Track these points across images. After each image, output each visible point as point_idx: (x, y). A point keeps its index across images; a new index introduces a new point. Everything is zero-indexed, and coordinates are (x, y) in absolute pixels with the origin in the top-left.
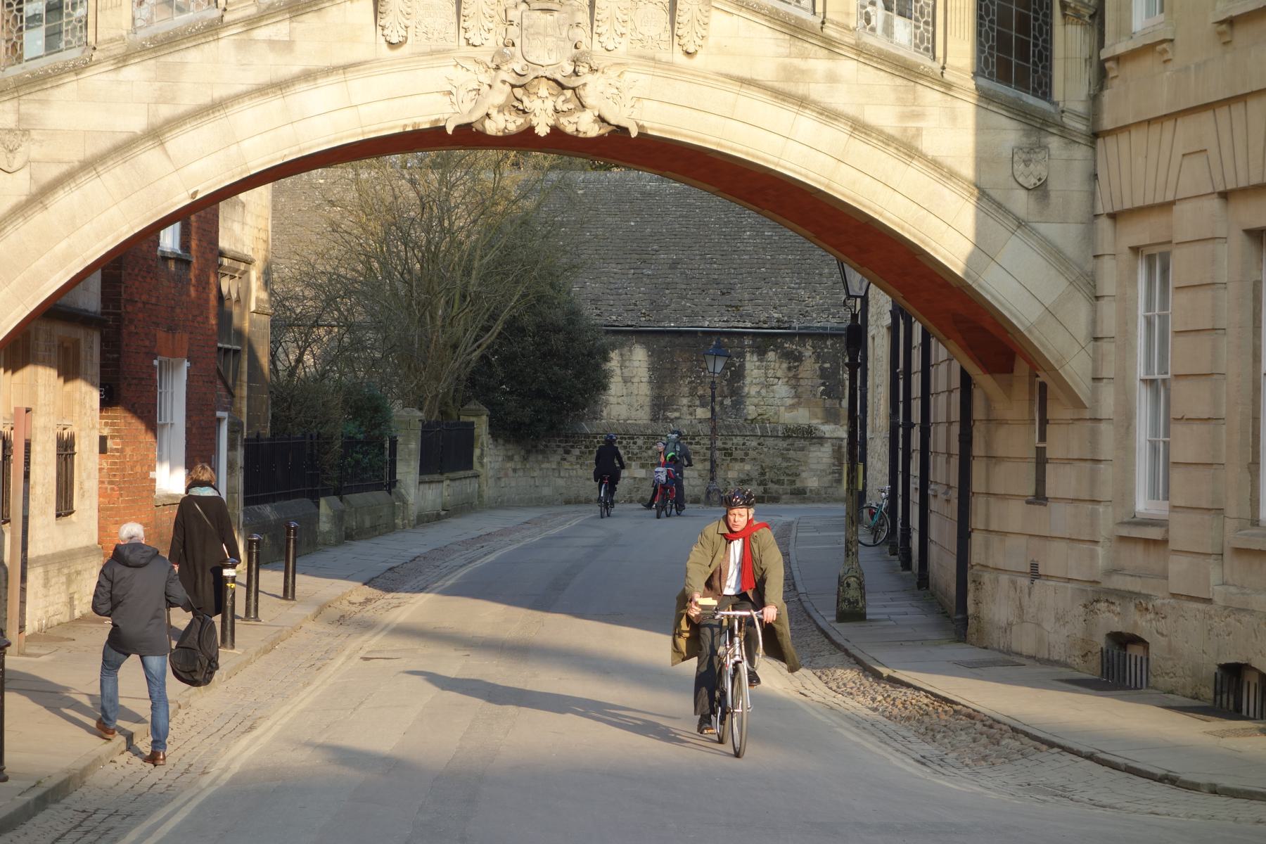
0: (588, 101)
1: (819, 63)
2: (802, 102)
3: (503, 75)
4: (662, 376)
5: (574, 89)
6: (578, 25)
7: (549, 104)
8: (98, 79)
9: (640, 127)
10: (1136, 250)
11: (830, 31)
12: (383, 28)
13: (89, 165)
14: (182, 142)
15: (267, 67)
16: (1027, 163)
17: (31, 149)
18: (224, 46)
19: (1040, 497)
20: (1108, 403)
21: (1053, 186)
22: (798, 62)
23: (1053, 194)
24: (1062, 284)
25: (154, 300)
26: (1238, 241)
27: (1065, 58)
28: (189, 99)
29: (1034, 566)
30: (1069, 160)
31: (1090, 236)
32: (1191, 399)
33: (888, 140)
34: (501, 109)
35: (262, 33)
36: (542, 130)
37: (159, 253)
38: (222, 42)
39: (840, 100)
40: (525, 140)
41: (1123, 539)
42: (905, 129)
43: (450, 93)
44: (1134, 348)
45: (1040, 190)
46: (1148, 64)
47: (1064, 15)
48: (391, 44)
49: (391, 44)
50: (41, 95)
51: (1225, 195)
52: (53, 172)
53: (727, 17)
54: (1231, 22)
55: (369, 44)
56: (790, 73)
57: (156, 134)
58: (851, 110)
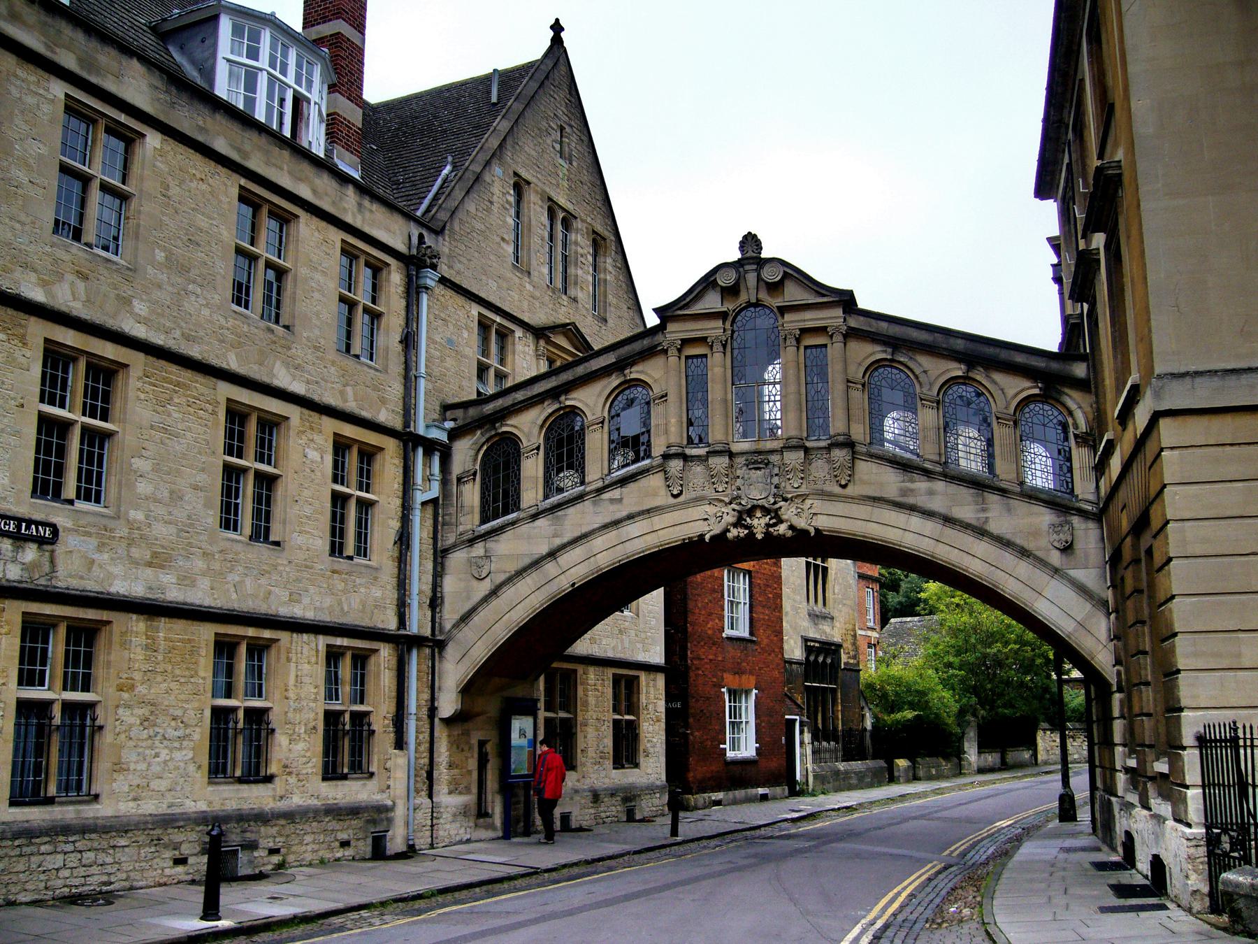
0: (784, 517)
1: (922, 485)
2: (912, 508)
3: (733, 506)
5: (776, 511)
6: (776, 475)
8: (524, 529)
9: (817, 530)
11: (928, 465)
12: (669, 486)
13: (520, 573)
14: (566, 559)
15: (607, 512)
16: (1058, 533)
18: (587, 505)
21: (1078, 546)
23: (1077, 552)
25: (720, 659)
30: (1087, 529)
34: (735, 525)
35: (606, 496)
36: (759, 536)
37: (724, 635)
39: (936, 505)
42: (978, 519)
43: (706, 519)
45: (1067, 549)
47: (1077, 442)
50: (496, 538)
52: (501, 578)
53: (862, 463)
55: (663, 499)
57: (552, 554)
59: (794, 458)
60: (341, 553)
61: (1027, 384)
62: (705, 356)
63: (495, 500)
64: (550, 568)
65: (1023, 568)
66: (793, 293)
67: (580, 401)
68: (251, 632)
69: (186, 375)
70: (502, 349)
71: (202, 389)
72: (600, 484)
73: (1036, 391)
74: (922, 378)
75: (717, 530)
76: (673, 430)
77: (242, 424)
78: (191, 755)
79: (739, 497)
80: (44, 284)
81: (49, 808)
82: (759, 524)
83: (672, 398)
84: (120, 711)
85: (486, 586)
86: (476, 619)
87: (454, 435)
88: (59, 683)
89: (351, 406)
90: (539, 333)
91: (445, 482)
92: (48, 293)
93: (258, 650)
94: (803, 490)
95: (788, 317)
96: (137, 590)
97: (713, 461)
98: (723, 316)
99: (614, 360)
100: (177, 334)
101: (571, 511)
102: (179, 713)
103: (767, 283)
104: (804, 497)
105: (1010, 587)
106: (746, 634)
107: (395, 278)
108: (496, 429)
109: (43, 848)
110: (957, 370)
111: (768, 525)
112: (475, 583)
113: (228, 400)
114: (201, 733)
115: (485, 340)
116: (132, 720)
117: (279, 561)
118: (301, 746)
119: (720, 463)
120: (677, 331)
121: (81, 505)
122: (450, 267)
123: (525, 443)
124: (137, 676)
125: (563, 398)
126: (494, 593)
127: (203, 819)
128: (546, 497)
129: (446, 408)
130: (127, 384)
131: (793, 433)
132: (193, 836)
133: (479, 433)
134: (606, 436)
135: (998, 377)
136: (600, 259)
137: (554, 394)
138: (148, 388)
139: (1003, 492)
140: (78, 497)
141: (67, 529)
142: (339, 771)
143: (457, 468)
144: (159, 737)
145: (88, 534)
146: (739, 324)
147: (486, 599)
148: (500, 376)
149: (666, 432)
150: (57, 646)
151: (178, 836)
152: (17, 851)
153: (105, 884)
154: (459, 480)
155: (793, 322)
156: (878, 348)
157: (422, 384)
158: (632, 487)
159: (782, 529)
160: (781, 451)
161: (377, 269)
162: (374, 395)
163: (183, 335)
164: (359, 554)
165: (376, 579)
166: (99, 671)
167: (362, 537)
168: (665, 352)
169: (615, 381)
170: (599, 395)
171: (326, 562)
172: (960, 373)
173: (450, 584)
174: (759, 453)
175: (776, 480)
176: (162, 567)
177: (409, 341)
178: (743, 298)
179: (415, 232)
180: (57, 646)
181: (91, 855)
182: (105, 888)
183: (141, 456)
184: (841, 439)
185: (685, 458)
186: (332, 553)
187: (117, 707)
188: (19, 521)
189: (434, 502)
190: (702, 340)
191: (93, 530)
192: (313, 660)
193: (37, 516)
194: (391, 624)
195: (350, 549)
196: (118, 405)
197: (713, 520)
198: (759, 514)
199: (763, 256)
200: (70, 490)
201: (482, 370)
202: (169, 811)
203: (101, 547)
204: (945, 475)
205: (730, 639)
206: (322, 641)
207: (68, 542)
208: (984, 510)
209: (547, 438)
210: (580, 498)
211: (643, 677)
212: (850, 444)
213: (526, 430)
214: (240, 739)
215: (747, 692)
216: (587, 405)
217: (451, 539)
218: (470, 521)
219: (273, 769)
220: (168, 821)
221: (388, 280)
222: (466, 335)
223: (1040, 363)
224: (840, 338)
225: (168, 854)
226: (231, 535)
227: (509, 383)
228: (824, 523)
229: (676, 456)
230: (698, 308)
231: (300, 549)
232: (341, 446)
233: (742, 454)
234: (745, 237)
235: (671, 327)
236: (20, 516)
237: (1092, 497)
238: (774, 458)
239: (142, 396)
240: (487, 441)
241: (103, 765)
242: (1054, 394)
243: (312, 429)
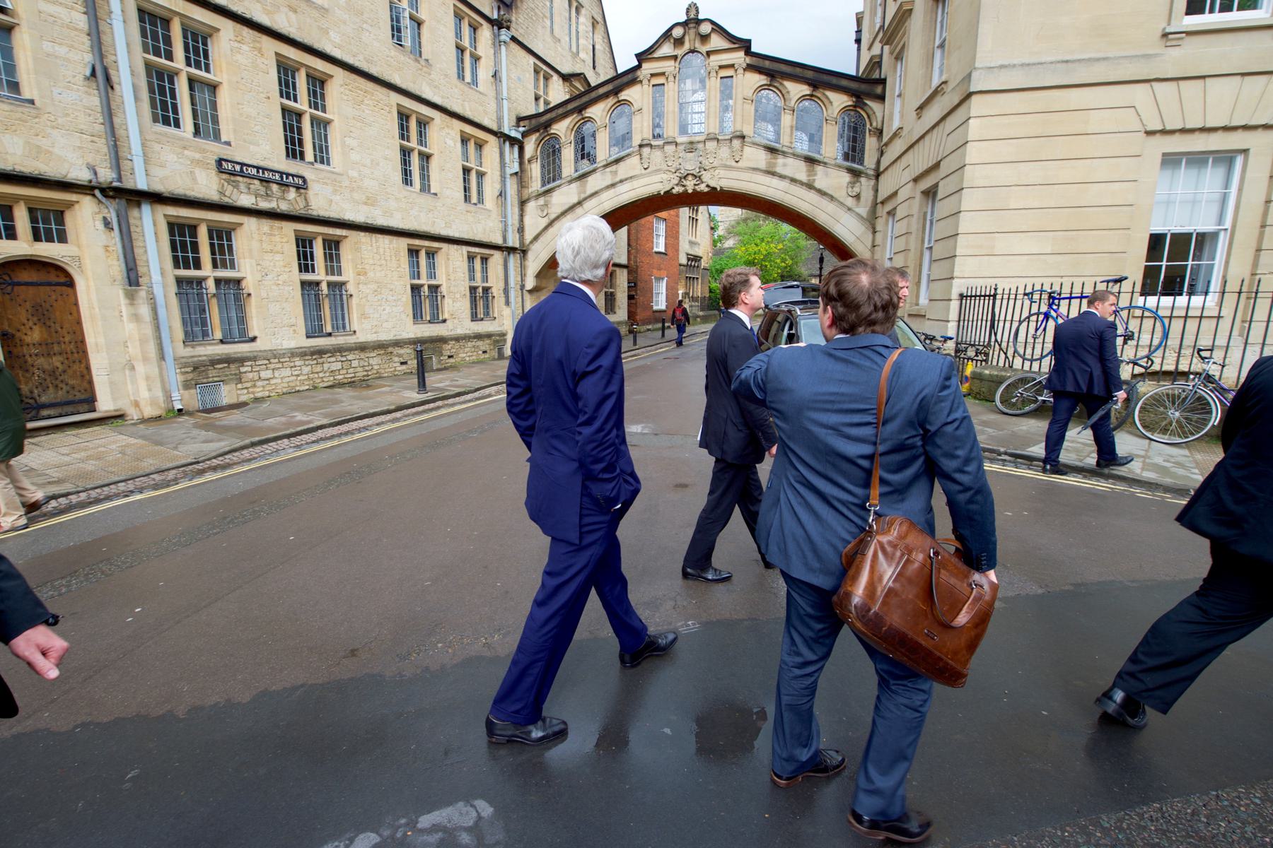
0: (704, 180)
2: (773, 174)
3: (677, 174)
8: (564, 189)
22: (773, 161)
28: (588, 193)
33: (802, 183)
34: (677, 185)
35: (608, 170)
36: (690, 191)
38: (598, 174)
48: (645, 169)
49: (645, 169)
55: (638, 170)
56: (769, 164)
57: (580, 203)
58: (790, 175)
59: (711, 145)
60: (470, 201)
63: (549, 173)
65: (830, 207)
68: (427, 243)
69: (370, 86)
70: (546, 86)
71: (381, 96)
72: (605, 163)
76: (645, 130)
77: (407, 122)
78: (402, 309)
79: (680, 169)
81: (329, 338)
82: (690, 185)
83: (645, 110)
84: (361, 286)
86: (542, 239)
87: (524, 135)
88: (323, 271)
89: (468, 114)
90: (566, 78)
91: (521, 163)
93: (431, 254)
94: (713, 165)
96: (359, 218)
97: (667, 148)
98: (675, 58)
100: (361, 58)
102: (392, 287)
109: (329, 360)
111: (695, 185)
113: (398, 104)
115: (537, 80)
116: (368, 291)
117: (437, 204)
118: (458, 305)
119: (670, 149)
120: (648, 68)
121: (318, 166)
122: (516, 30)
123: (563, 139)
124: (367, 267)
127: (414, 342)
128: (576, 171)
129: (520, 119)
131: (711, 130)
132: (408, 351)
133: (538, 134)
134: (607, 135)
136: (596, 36)
138: (347, 92)
140: (316, 161)
141: (313, 181)
142: (479, 316)
144: (384, 300)
145: (327, 184)
147: (546, 228)
148: (547, 103)
149: (642, 132)
150: (318, 250)
151: (402, 351)
152: (315, 362)
153: (364, 376)
158: (622, 164)
159: (703, 188)
161: (474, 28)
162: (481, 108)
164: (479, 202)
165: (489, 216)
166: (344, 264)
167: (480, 193)
168: (641, 82)
169: (611, 101)
170: (603, 111)
171: (462, 205)
173: (527, 220)
174: (691, 143)
176: (372, 205)
180: (318, 250)
181: (357, 362)
182: (366, 378)
183: (350, 137)
184: (738, 134)
185: (651, 146)
186: (466, 200)
187: (358, 284)
188: (281, 173)
189: (516, 173)
190: (663, 74)
191: (329, 182)
192: (461, 259)
195: (474, 199)
197: (665, 182)
198: (690, 178)
200: (309, 155)
201: (537, 99)
202: (395, 338)
203: (335, 191)
204: (794, 155)
206: (465, 249)
209: (575, 137)
212: (743, 137)
214: (427, 301)
216: (597, 116)
217: (525, 197)
218: (535, 185)
219: (446, 316)
220: (398, 344)
222: (527, 75)
223: (853, 85)
226: (409, 188)
227: (552, 105)
229: (647, 145)
230: (658, 54)
231: (448, 197)
232: (465, 140)
233: (682, 144)
235: (645, 65)
236: (281, 170)
238: (700, 146)
239: (345, 98)
243: (448, 126)
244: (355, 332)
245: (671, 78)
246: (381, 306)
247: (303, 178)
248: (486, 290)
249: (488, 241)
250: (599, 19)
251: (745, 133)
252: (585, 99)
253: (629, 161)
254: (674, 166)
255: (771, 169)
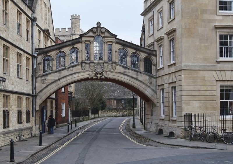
0: (104, 75)
1: (127, 71)
2: (126, 75)
4: (117, 103)
7: (99, 76)
8: (53, 74)
9: (109, 78)
10: (161, 89)
11: (129, 67)
14: (62, 80)
17: (46, 81)
18: (66, 71)
19: (152, 115)
20: (158, 105)
21: (152, 83)
22: (125, 71)
24: (153, 93)
26: (170, 88)
27: (153, 70)
28: (62, 76)
29: (152, 122)
31: (156, 88)
32: (166, 104)
34: (94, 76)
35: (70, 69)
36: (99, 78)
39: (130, 74)
40: (97, 79)
41: (160, 119)
44: (161, 99)
46: (161, 70)
51: (169, 83)
52: (48, 84)
54: (169, 66)
55: (81, 70)
56: (125, 72)
57: (59, 80)
58: (131, 75)
59: (106, 65)
61: (146, 54)
62: (89, 44)
64: (59, 82)
65: (143, 86)
66: (106, 34)
67: (64, 50)
68: (20, 96)
72: (69, 67)
73: (147, 56)
74: (128, 52)
75: (91, 77)
80: (3, 33)
82: (99, 76)
83: (83, 51)
85: (45, 85)
86: (43, 91)
87: (38, 55)
90: (44, 31)
92: (3, 36)
95: (105, 39)
98: (93, 37)
99: (71, 43)
101: (62, 71)
102: (15, 111)
103: (101, 31)
104: (107, 72)
105: (141, 89)
106: (63, 91)
107: (31, 24)
108: (47, 54)
109: (7, 136)
110: (134, 51)
111: (100, 76)
112: (43, 84)
114: (17, 115)
119: (92, 65)
120: (84, 39)
125: (61, 50)
126: (47, 86)
129: (36, 49)
130: (9, 51)
133: (43, 55)
135: (141, 53)
137: (59, 49)
139: (141, 73)
143: (38, 62)
146: (95, 39)
147: (45, 88)
149: (82, 58)
154: (39, 64)
155: (106, 39)
156: (121, 46)
157: (34, 44)
158: (75, 67)
160: (103, 63)
163: (14, 40)
168: (82, 43)
172: (135, 52)
173: (37, 84)
174: (99, 63)
175: (102, 68)
177: (32, 37)
178: (97, 34)
179: (32, 13)
193: (4, 77)
194: (31, 93)
196: (8, 55)
199: (101, 26)
204: (132, 69)
205: (62, 92)
207: (7, 81)
208: (138, 76)
210: (64, 69)
211: (53, 100)
212: (116, 63)
213: (53, 55)
215: (64, 103)
216: (66, 51)
218: (41, 72)
221: (29, 24)
224: (114, 43)
225: (16, 137)
228: (110, 76)
230: (88, 35)
233: (96, 63)
234: (98, 22)
235: (83, 38)
237: (155, 75)
239: (11, 53)
240: (45, 56)
241: (9, 121)
242: (150, 57)
244: (9, 127)
245: (92, 43)
246: (13, 118)
247: (5, 79)
248: (28, 110)
249: (29, 93)
250: (50, 8)
251: (116, 61)
252: (61, 45)
253: (77, 67)
254: (93, 70)
255: (124, 73)
